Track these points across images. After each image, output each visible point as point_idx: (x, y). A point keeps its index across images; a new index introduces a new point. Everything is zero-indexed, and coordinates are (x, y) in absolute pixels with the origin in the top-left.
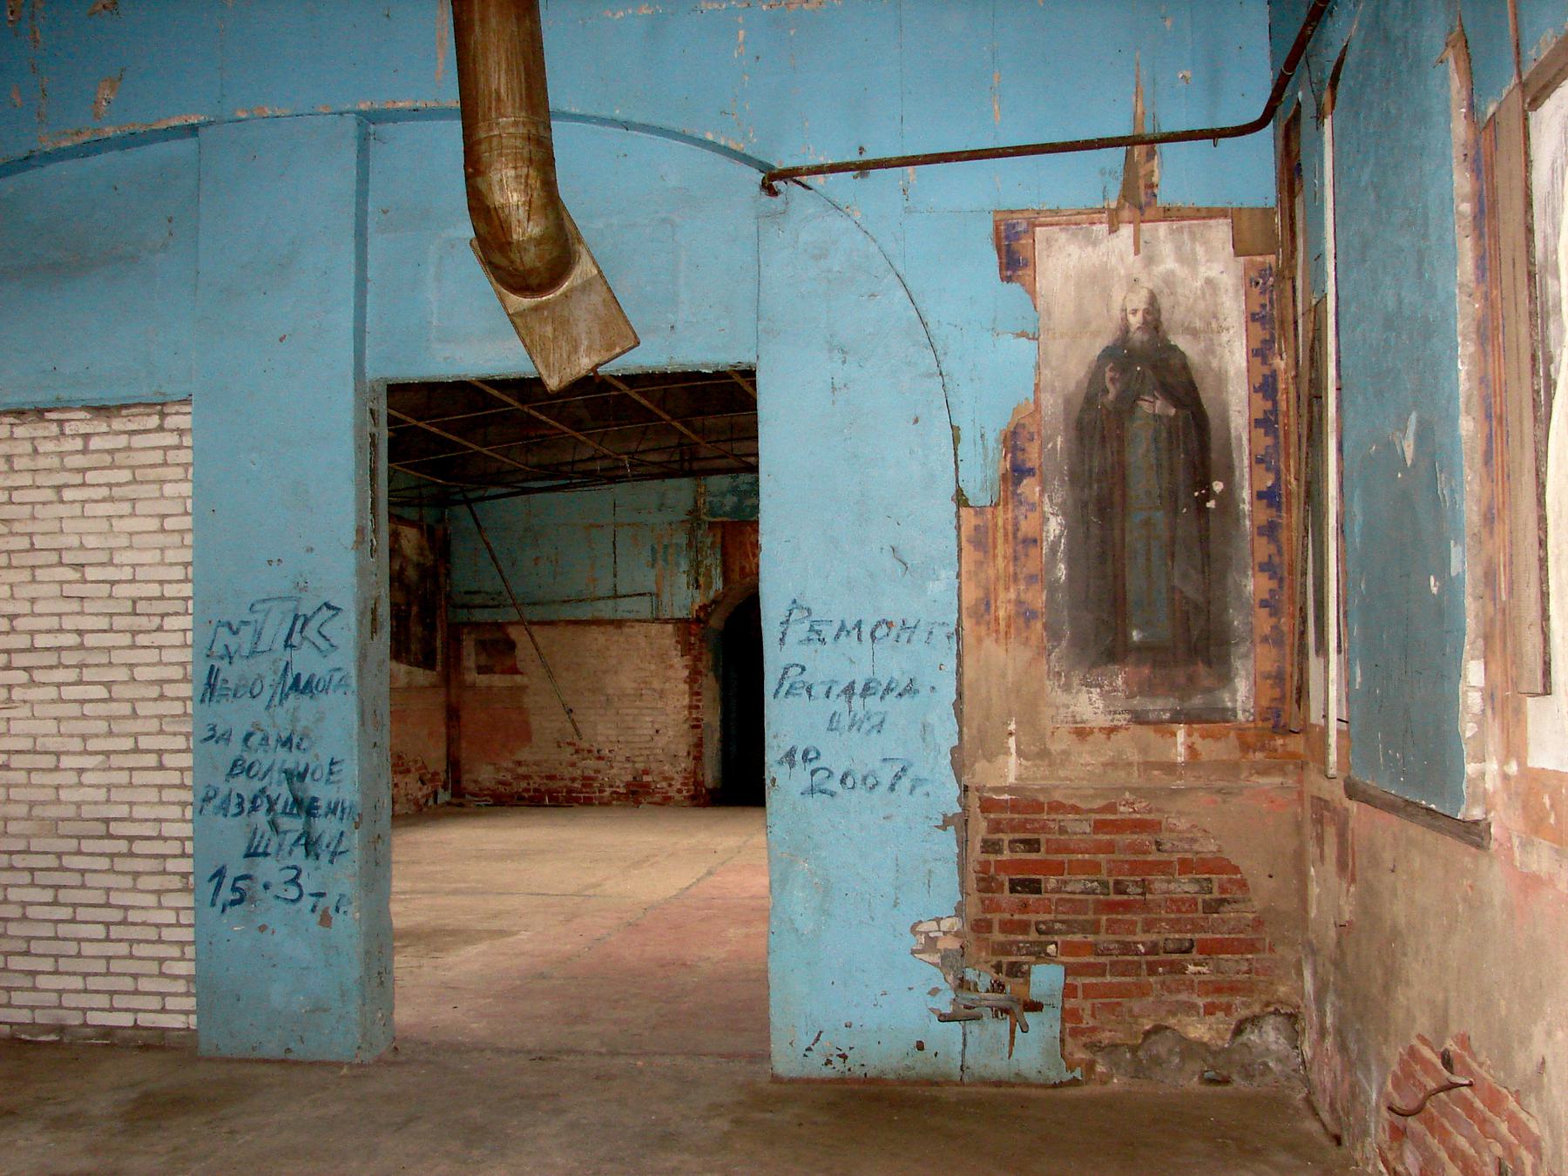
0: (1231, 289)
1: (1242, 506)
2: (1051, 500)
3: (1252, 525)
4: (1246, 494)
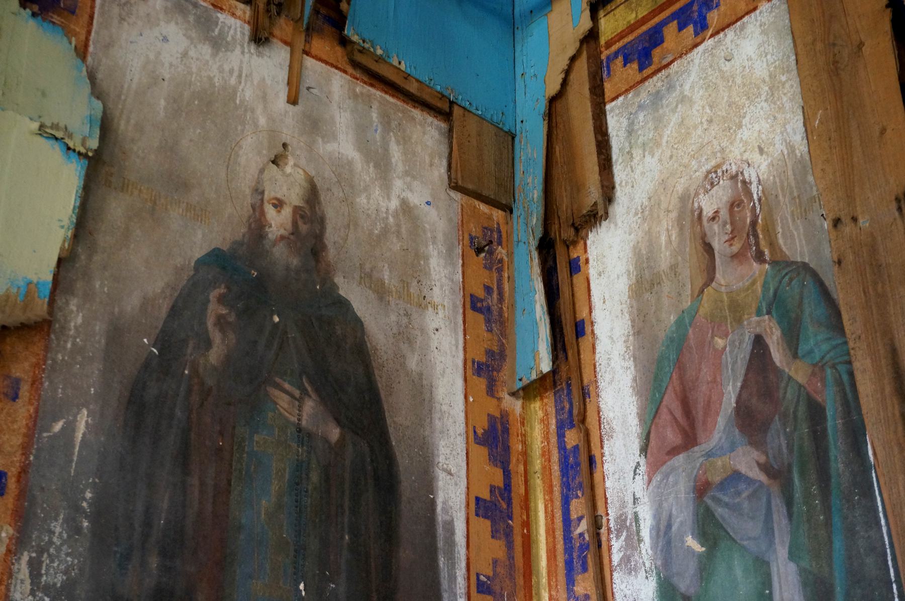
0: (440, 237)
2: (35, 574)
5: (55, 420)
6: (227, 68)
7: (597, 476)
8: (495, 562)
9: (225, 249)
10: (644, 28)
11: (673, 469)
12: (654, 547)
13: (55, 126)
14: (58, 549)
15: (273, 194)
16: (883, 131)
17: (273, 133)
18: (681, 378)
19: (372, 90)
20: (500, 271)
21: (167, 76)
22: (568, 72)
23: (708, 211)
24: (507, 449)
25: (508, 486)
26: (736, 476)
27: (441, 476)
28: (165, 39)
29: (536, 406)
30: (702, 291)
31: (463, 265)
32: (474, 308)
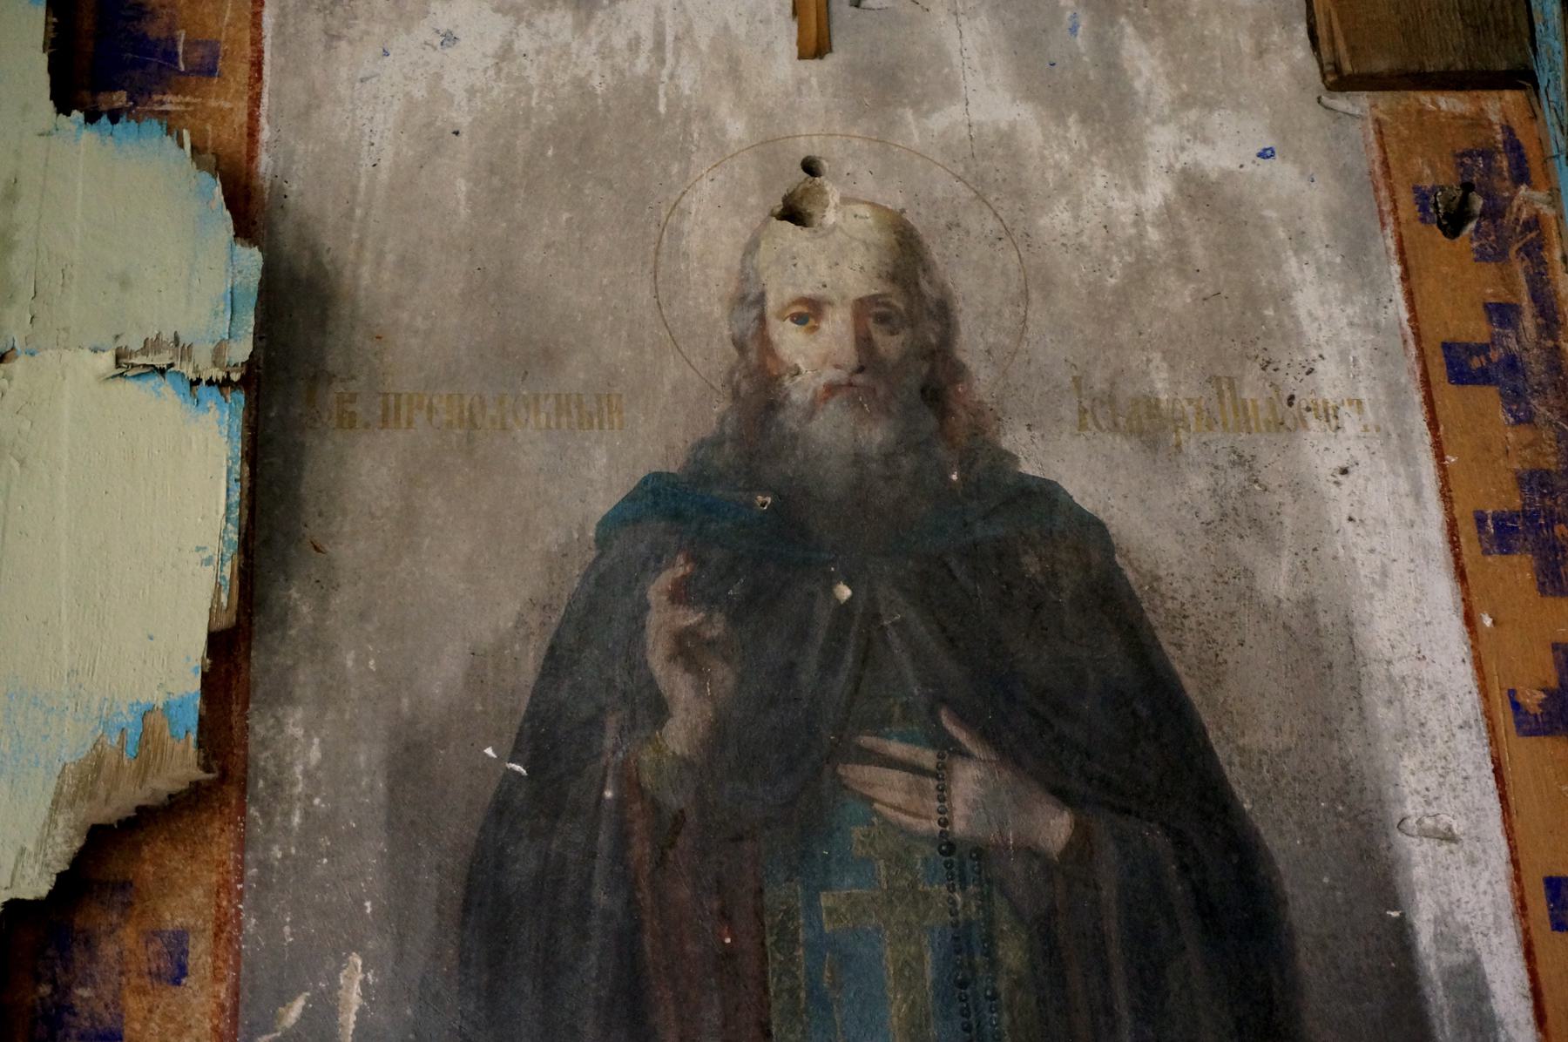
0: (1318, 227)
5: (284, 998)
6: (619, 41)
9: (673, 469)
13: (152, 346)
15: (790, 293)
17: (767, 147)
20: (1534, 251)
21: (463, 120)
31: (1405, 277)
32: (1460, 374)
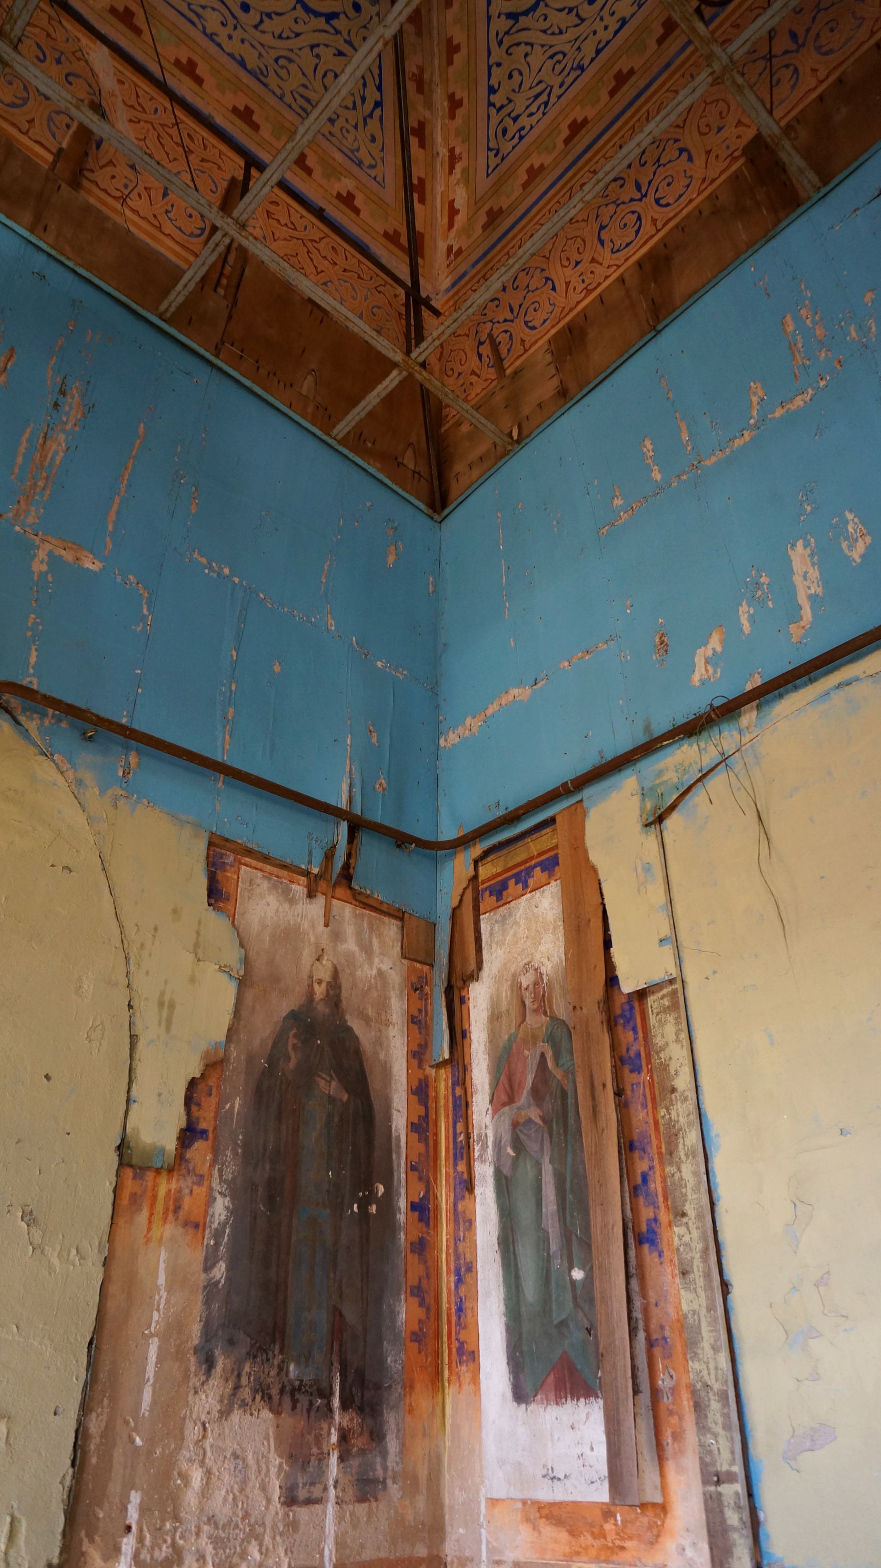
0: (397, 986)
1: (398, 1216)
2: (221, 1176)
3: (406, 1239)
4: (402, 1203)
7: (469, 1112)
8: (420, 1155)
10: (500, 878)
11: (504, 1114)
12: (493, 1151)
13: (225, 966)
14: (229, 1163)
16: (595, 967)
17: (317, 944)
18: (509, 1067)
19: (364, 911)
20: (426, 999)
21: (269, 924)
22: (462, 896)
23: (524, 985)
24: (427, 1096)
25: (427, 1115)
26: (529, 1121)
27: (395, 1113)
28: (268, 905)
29: (442, 1071)
30: (520, 1026)
32: (413, 1022)
